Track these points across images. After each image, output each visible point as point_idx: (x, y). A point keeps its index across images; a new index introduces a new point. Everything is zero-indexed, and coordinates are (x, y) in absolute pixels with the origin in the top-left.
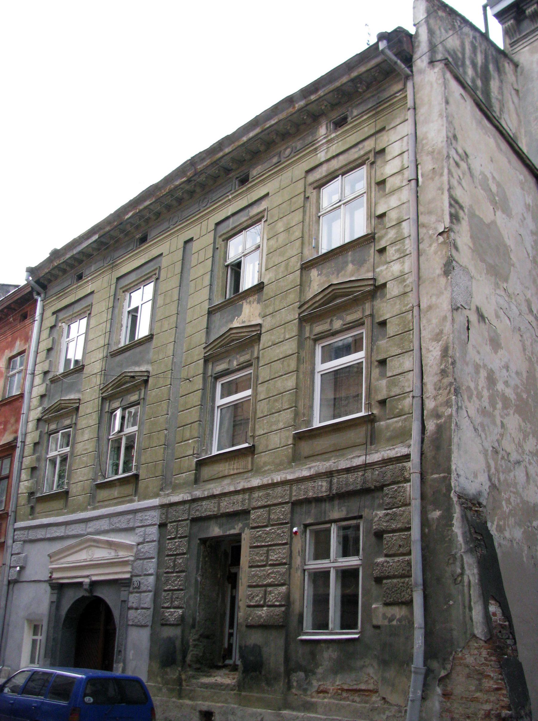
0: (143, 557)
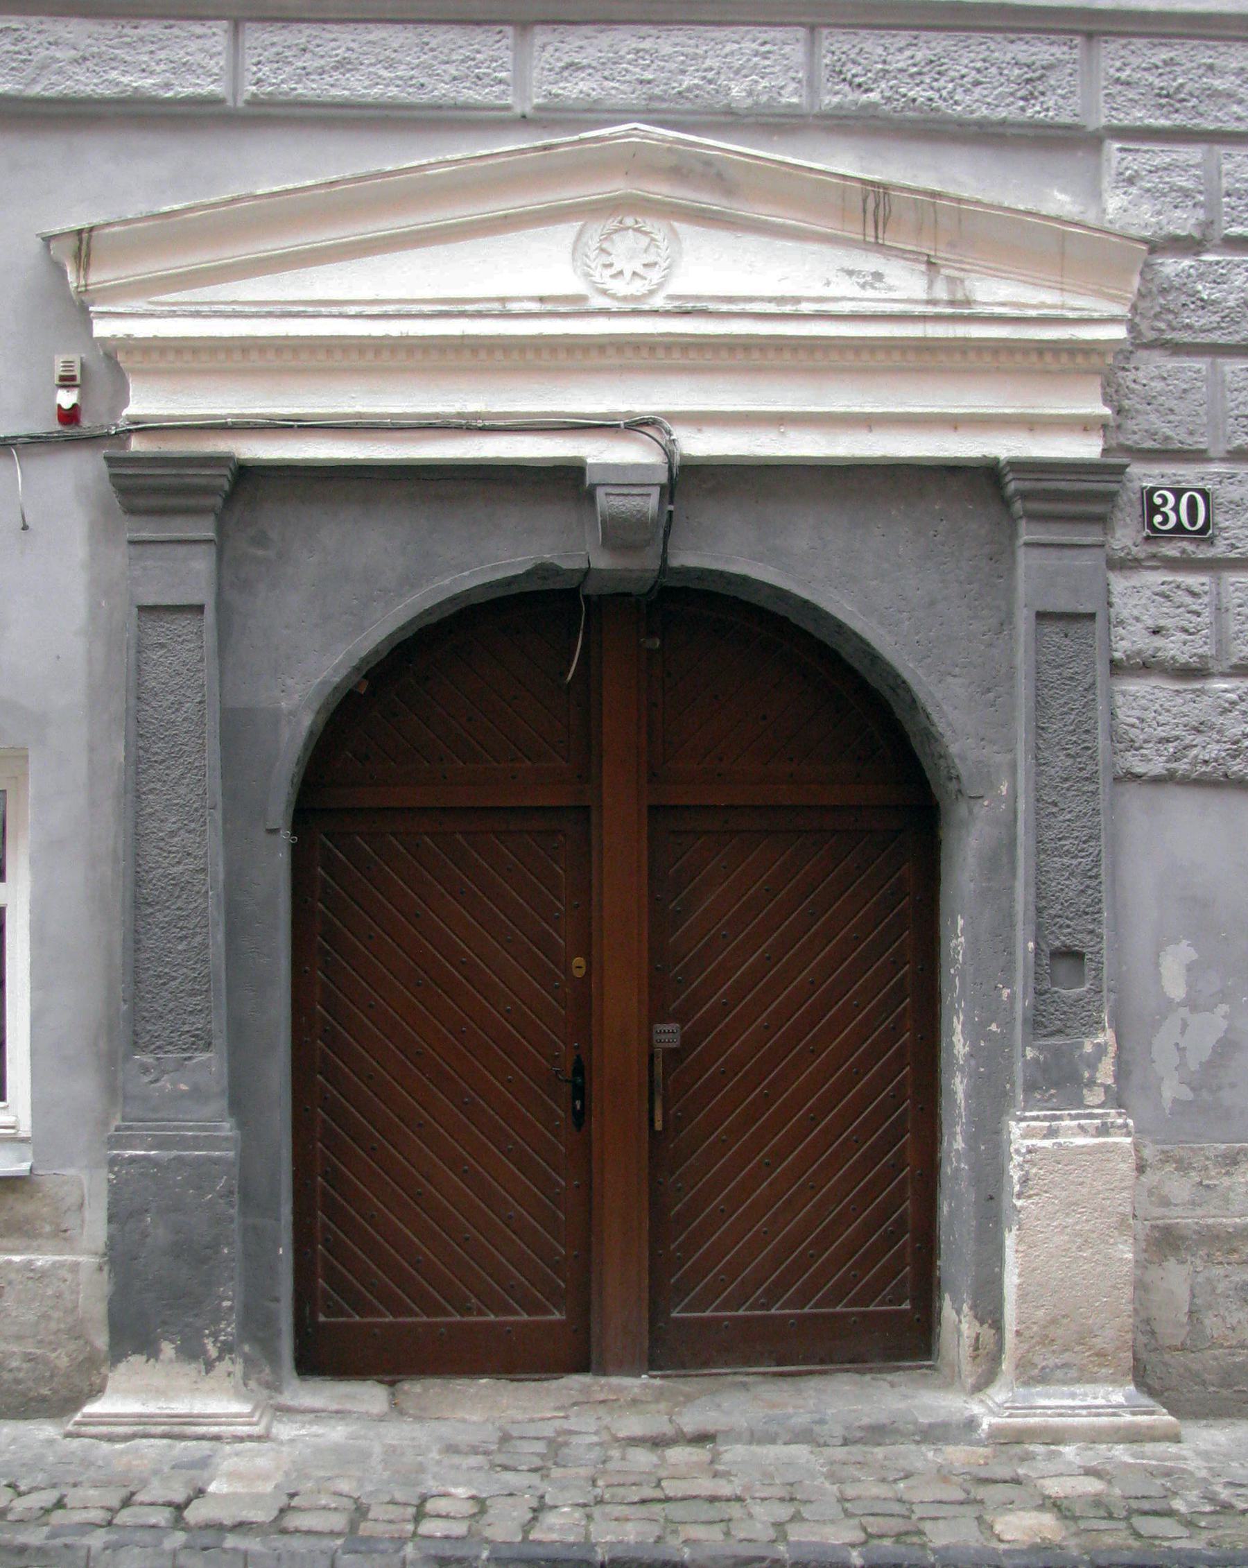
0: (1215, 337)
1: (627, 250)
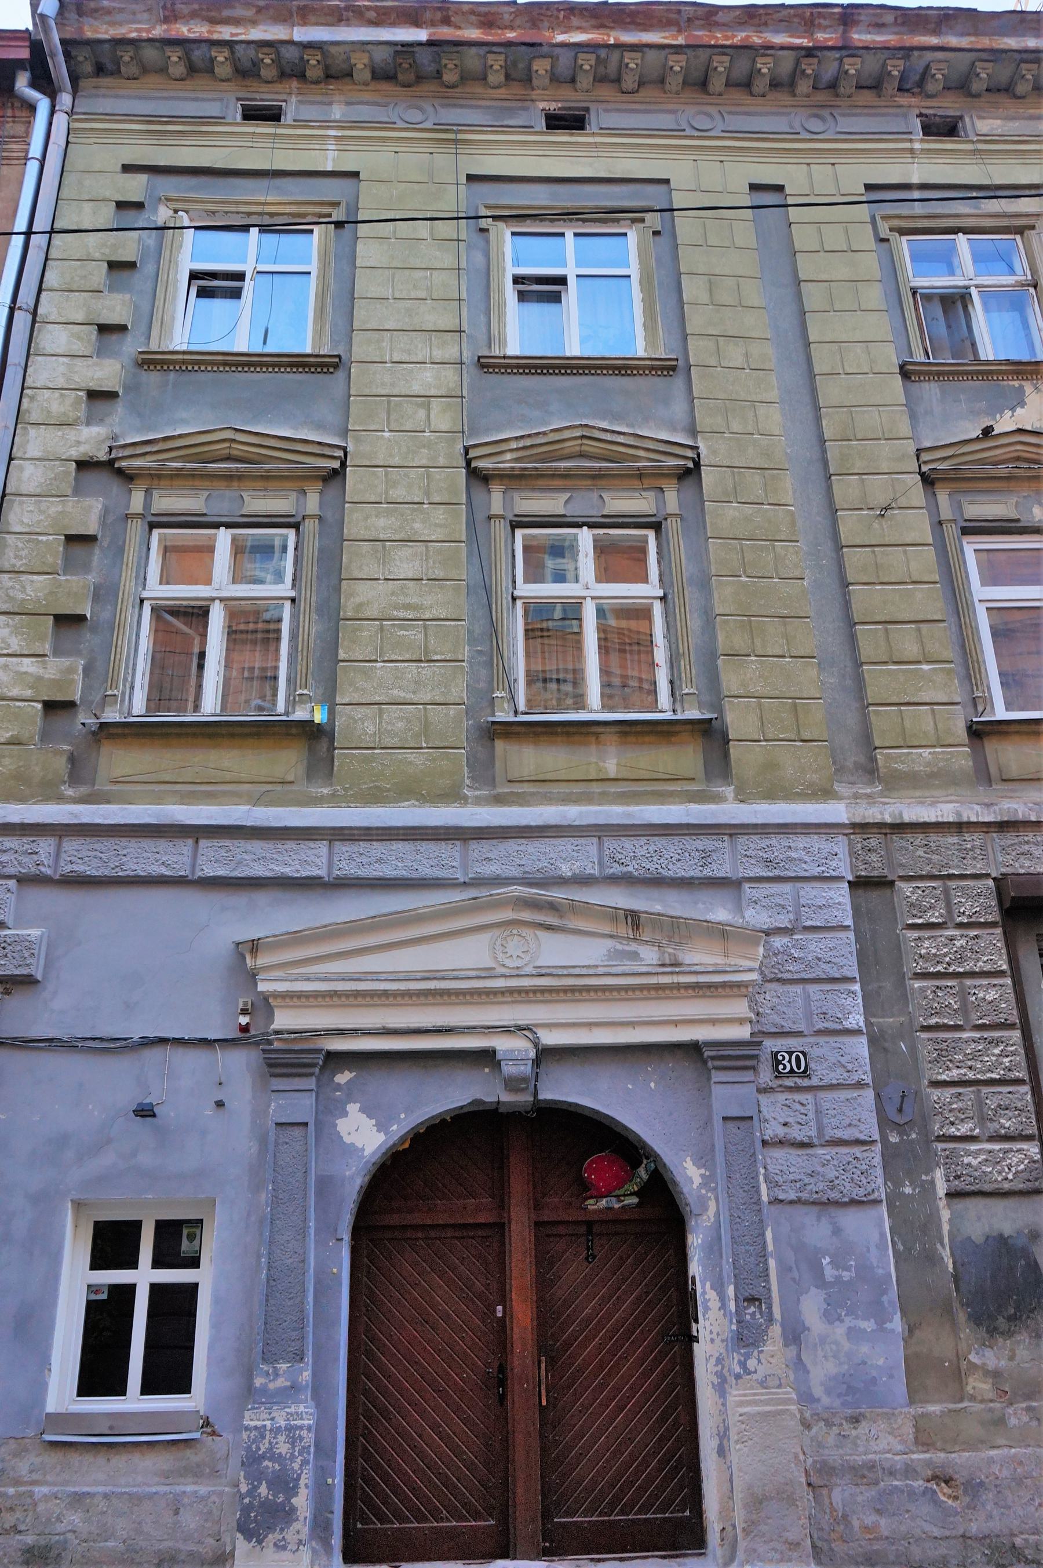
1: (514, 946)
